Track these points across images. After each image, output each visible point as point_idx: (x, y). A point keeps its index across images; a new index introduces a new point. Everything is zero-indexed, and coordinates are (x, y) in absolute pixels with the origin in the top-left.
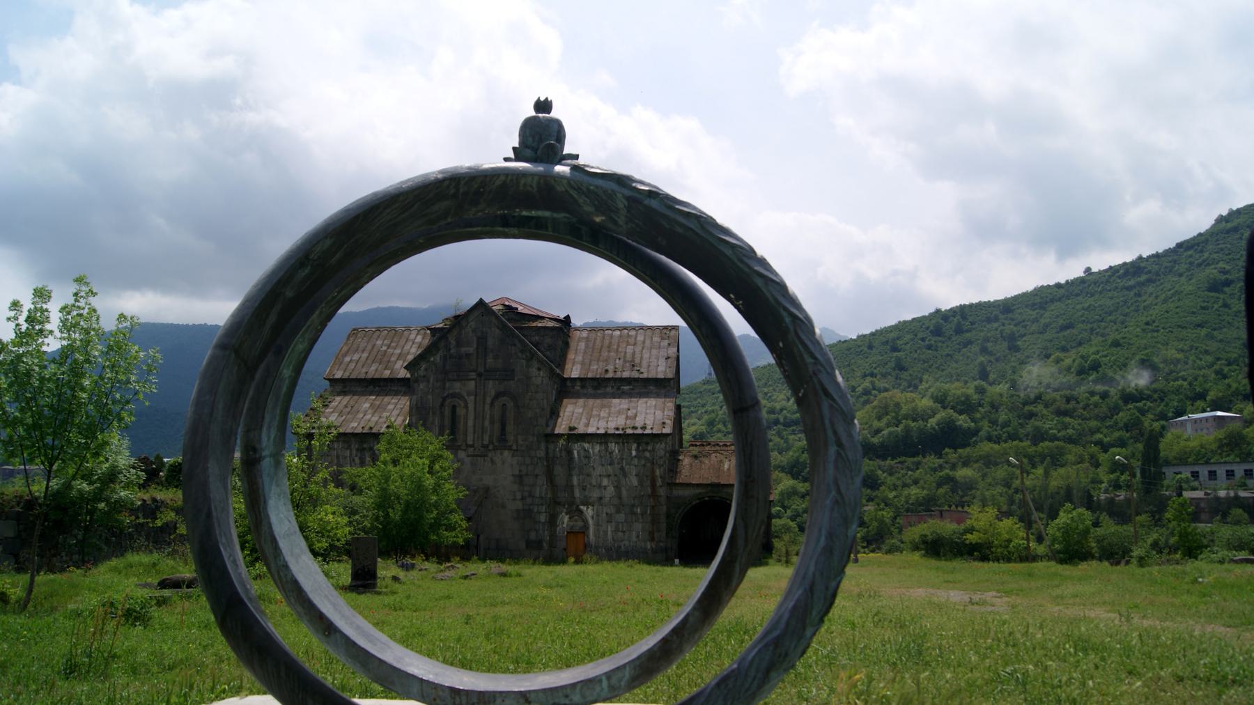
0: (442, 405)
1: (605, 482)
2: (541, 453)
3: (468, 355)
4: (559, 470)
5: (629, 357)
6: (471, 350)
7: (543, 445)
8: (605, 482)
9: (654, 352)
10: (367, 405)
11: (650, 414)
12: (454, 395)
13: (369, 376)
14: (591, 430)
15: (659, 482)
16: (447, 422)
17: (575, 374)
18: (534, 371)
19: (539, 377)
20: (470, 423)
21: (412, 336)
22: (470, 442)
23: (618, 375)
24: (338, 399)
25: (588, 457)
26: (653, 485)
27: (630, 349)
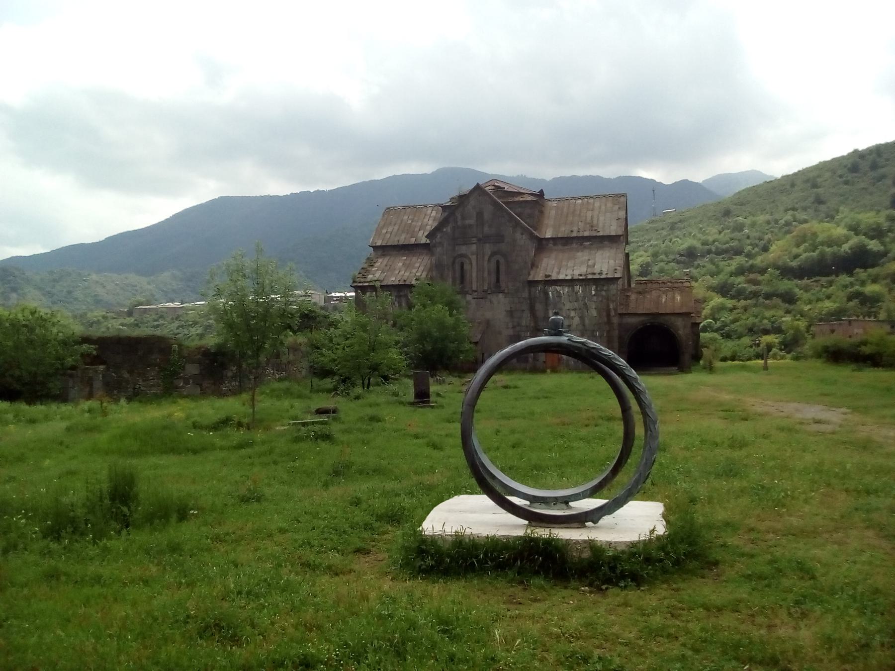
0: (454, 263)
1: (573, 314)
2: (526, 294)
3: (470, 226)
4: (539, 307)
5: (589, 219)
6: (471, 221)
7: (527, 290)
8: (573, 314)
9: (608, 215)
10: (400, 264)
11: (604, 263)
12: (462, 256)
13: (401, 243)
14: (561, 277)
15: (613, 313)
16: (458, 275)
17: (548, 236)
18: (518, 235)
19: (522, 239)
20: (474, 275)
21: (429, 212)
22: (474, 288)
23: (581, 234)
24: (380, 260)
25: (559, 296)
26: (608, 315)
27: (589, 214)
